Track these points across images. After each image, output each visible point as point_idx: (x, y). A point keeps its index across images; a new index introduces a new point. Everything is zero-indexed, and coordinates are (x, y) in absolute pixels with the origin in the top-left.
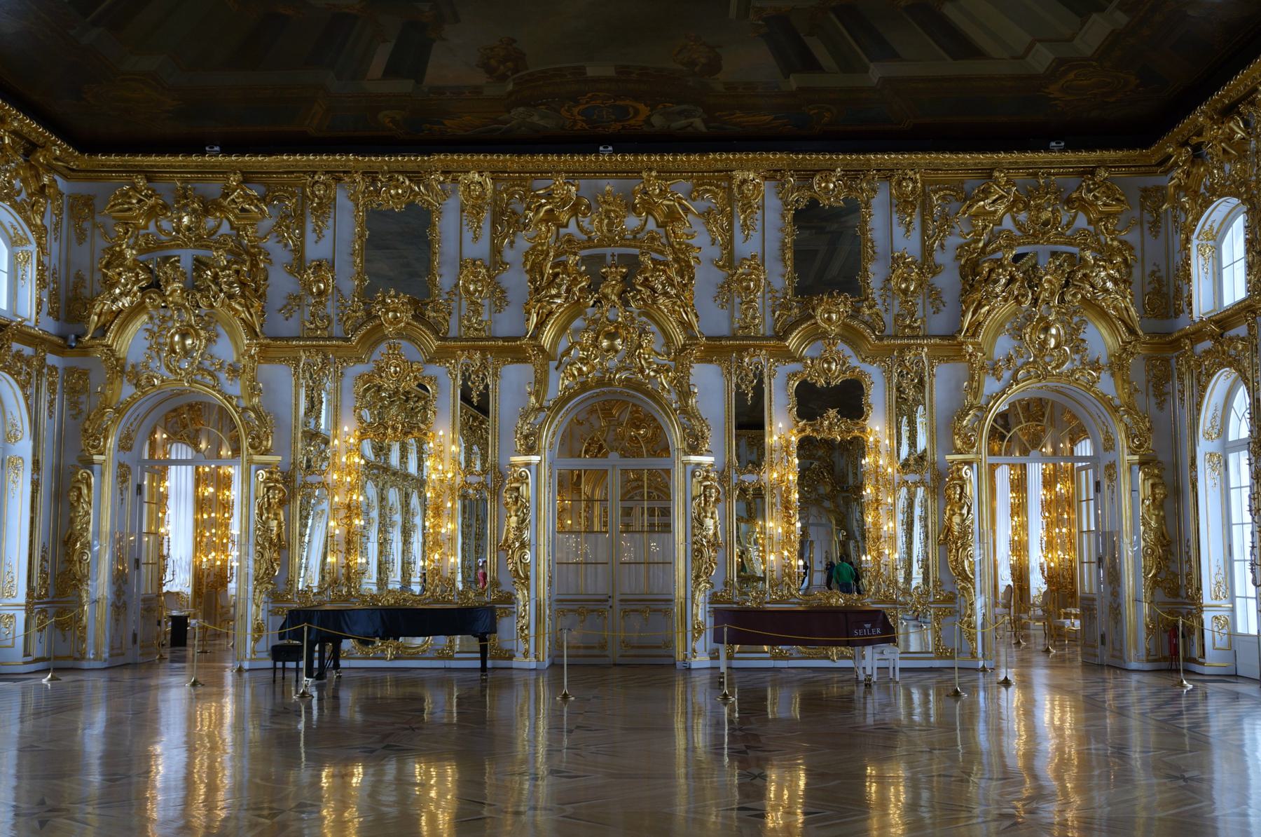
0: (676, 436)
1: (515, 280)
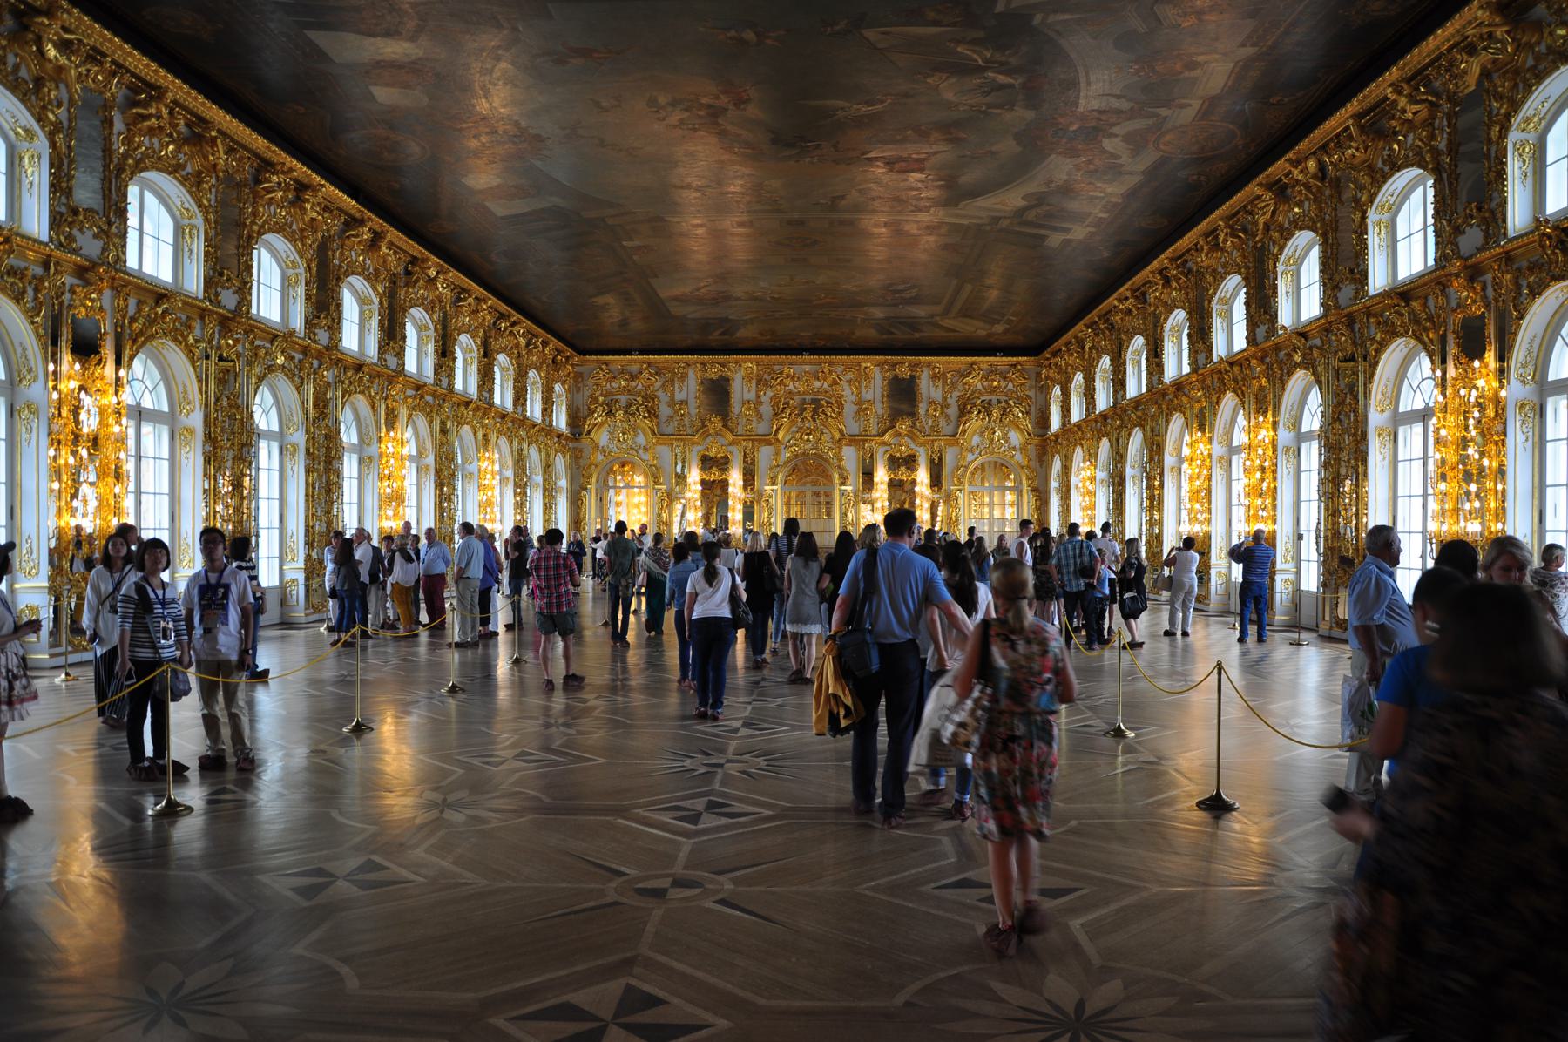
0: (836, 477)
1: (766, 409)
